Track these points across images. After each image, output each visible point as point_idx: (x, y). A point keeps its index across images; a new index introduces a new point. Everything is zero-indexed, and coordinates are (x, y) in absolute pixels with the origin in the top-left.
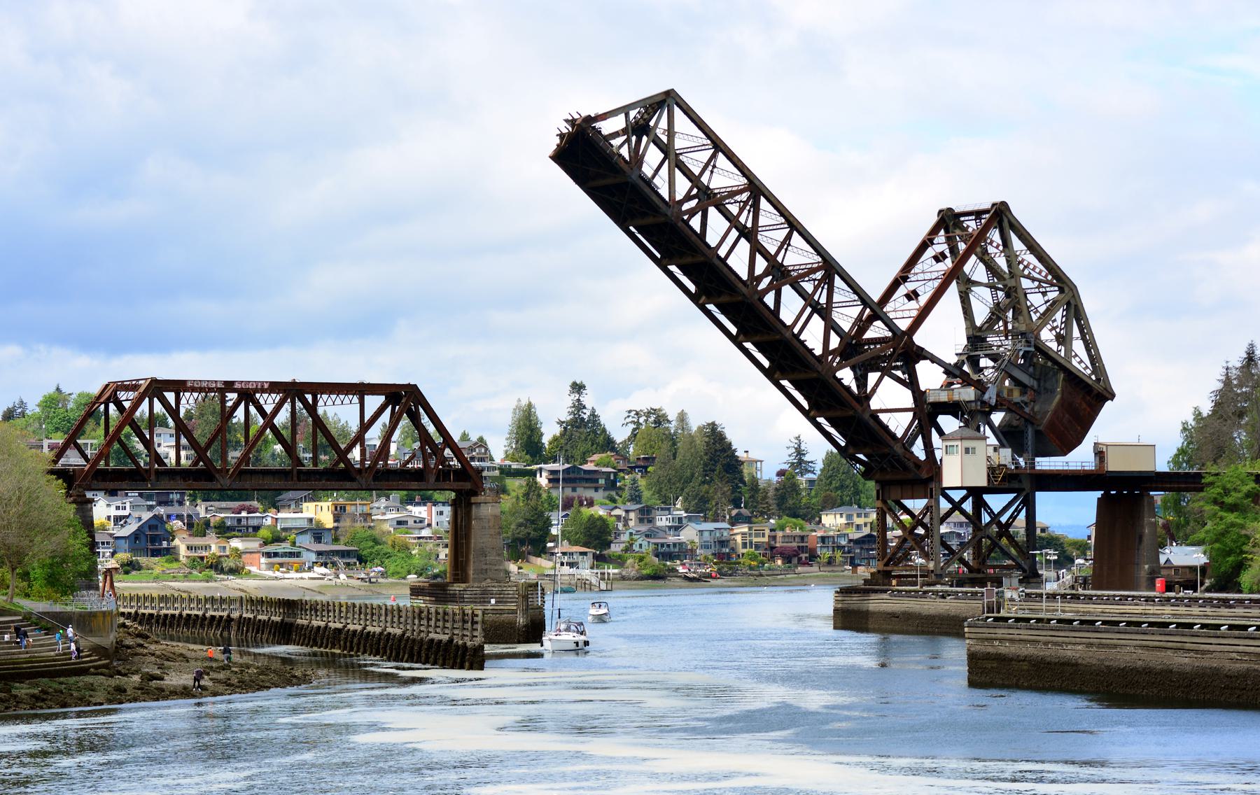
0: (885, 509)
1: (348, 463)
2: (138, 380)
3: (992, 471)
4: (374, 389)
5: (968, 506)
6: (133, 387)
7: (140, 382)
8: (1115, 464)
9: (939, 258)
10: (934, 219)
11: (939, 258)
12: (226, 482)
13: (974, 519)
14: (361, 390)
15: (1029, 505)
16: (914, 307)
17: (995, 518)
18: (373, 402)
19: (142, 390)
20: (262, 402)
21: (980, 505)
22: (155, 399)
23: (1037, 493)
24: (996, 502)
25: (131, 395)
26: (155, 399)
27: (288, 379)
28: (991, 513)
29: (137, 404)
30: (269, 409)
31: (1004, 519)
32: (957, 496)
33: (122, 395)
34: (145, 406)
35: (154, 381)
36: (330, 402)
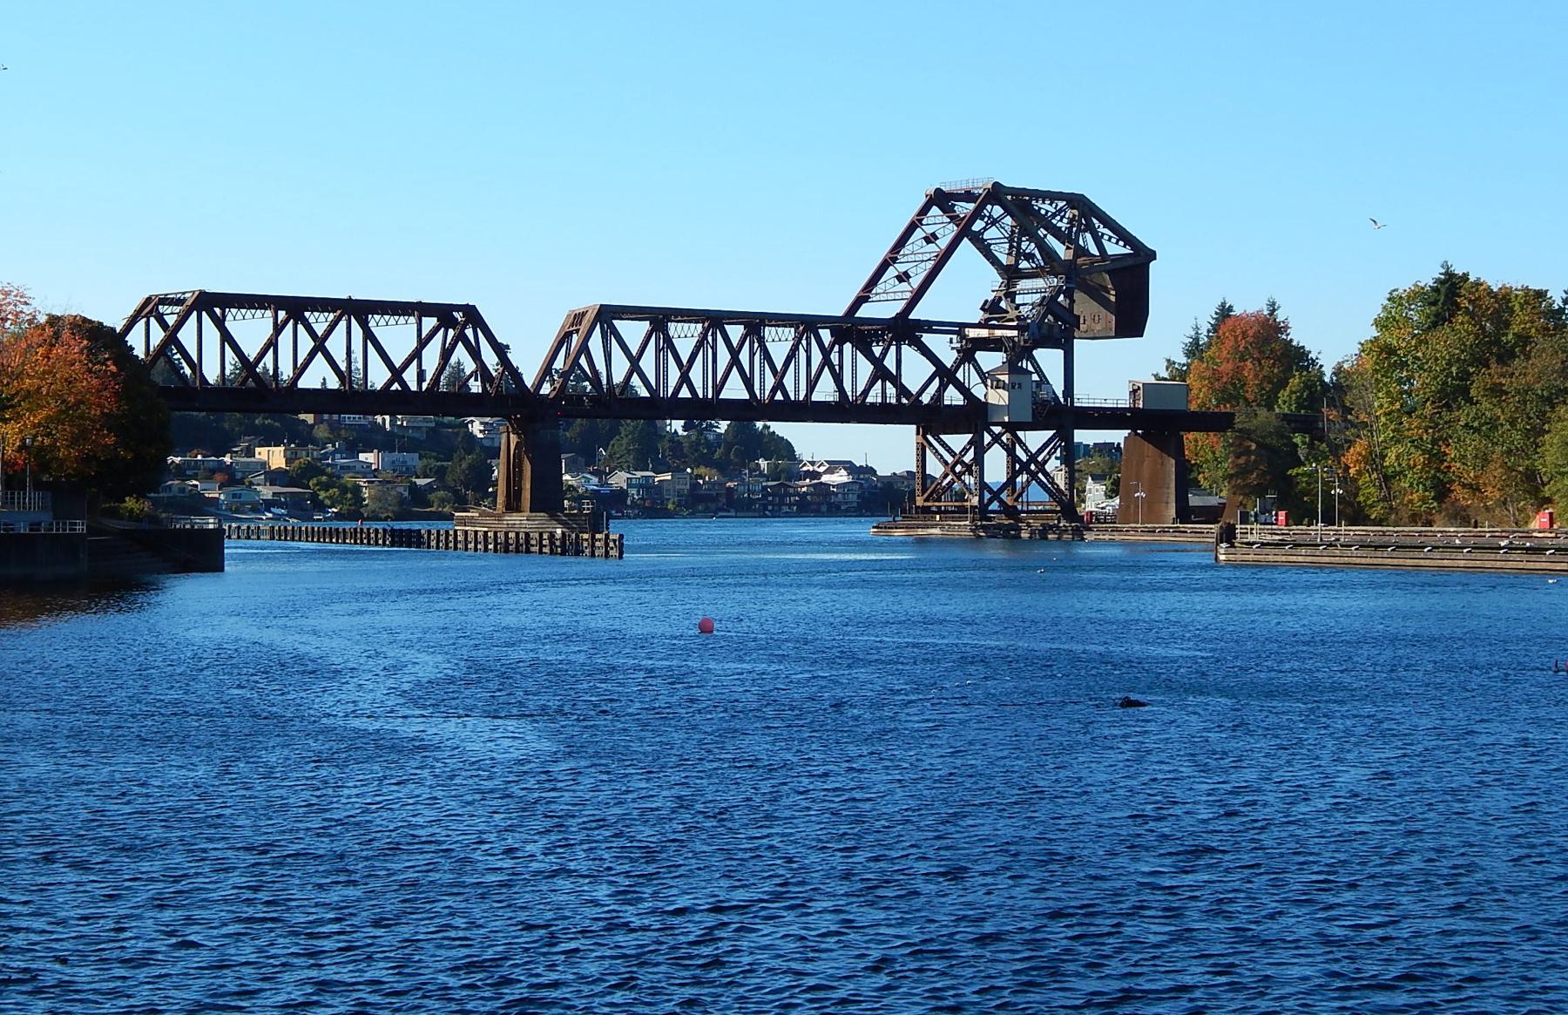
0: (925, 443)
2: (184, 293)
7: (187, 295)
10: (923, 200)
14: (419, 310)
17: (1033, 458)
19: (189, 303)
20: (312, 320)
22: (204, 313)
23: (1075, 431)
24: (1035, 439)
25: (177, 309)
26: (204, 313)
27: (345, 297)
28: (1026, 450)
30: (320, 329)
31: (1040, 459)
32: (997, 430)
35: (202, 294)
36: (382, 322)
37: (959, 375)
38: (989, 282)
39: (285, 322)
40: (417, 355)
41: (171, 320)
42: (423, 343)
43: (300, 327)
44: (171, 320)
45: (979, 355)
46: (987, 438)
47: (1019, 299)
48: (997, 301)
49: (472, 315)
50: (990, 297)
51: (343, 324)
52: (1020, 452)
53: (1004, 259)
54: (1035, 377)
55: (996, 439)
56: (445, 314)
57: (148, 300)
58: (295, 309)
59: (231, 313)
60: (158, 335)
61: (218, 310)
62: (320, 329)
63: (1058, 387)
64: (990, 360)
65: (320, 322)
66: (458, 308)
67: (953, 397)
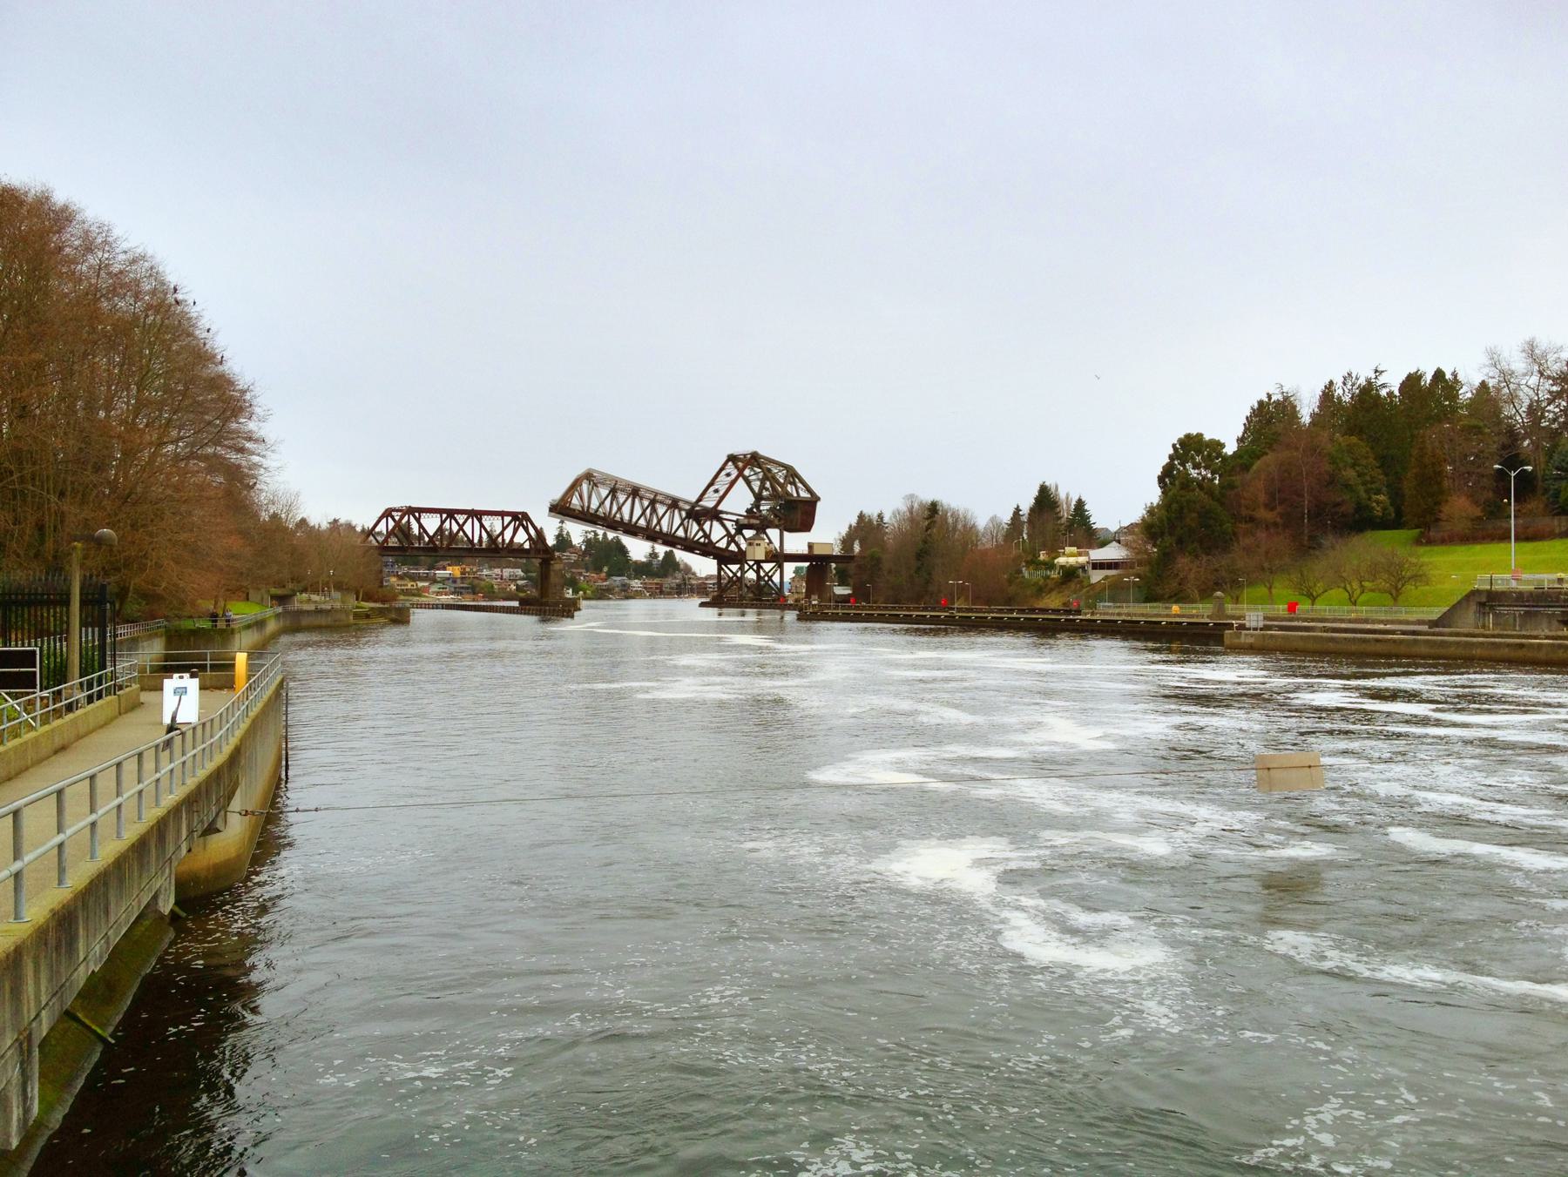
1: (496, 545)
3: (767, 553)
4: (508, 514)
5: (755, 567)
6: (398, 511)
8: (817, 552)
9: (728, 475)
11: (728, 475)
12: (441, 553)
13: (757, 572)
14: (502, 514)
15: (781, 567)
16: (717, 496)
17: (767, 574)
18: (507, 519)
21: (760, 567)
24: (767, 567)
25: (400, 514)
29: (402, 518)
30: (461, 522)
32: (751, 563)
33: (394, 513)
34: (406, 519)
37: (736, 539)
38: (749, 500)
39: (446, 519)
40: (502, 533)
41: (397, 518)
42: (504, 528)
43: (453, 521)
44: (397, 518)
45: (745, 532)
46: (746, 567)
47: (762, 508)
48: (752, 509)
49: (525, 516)
50: (750, 507)
51: (470, 520)
52: (762, 574)
53: (756, 489)
54: (767, 541)
55: (751, 567)
56: (515, 516)
57: (387, 510)
58: (451, 514)
59: (423, 515)
60: (391, 524)
61: (417, 514)
62: (461, 522)
63: (777, 545)
64: (749, 533)
65: (461, 519)
66: (520, 513)
67: (733, 547)
